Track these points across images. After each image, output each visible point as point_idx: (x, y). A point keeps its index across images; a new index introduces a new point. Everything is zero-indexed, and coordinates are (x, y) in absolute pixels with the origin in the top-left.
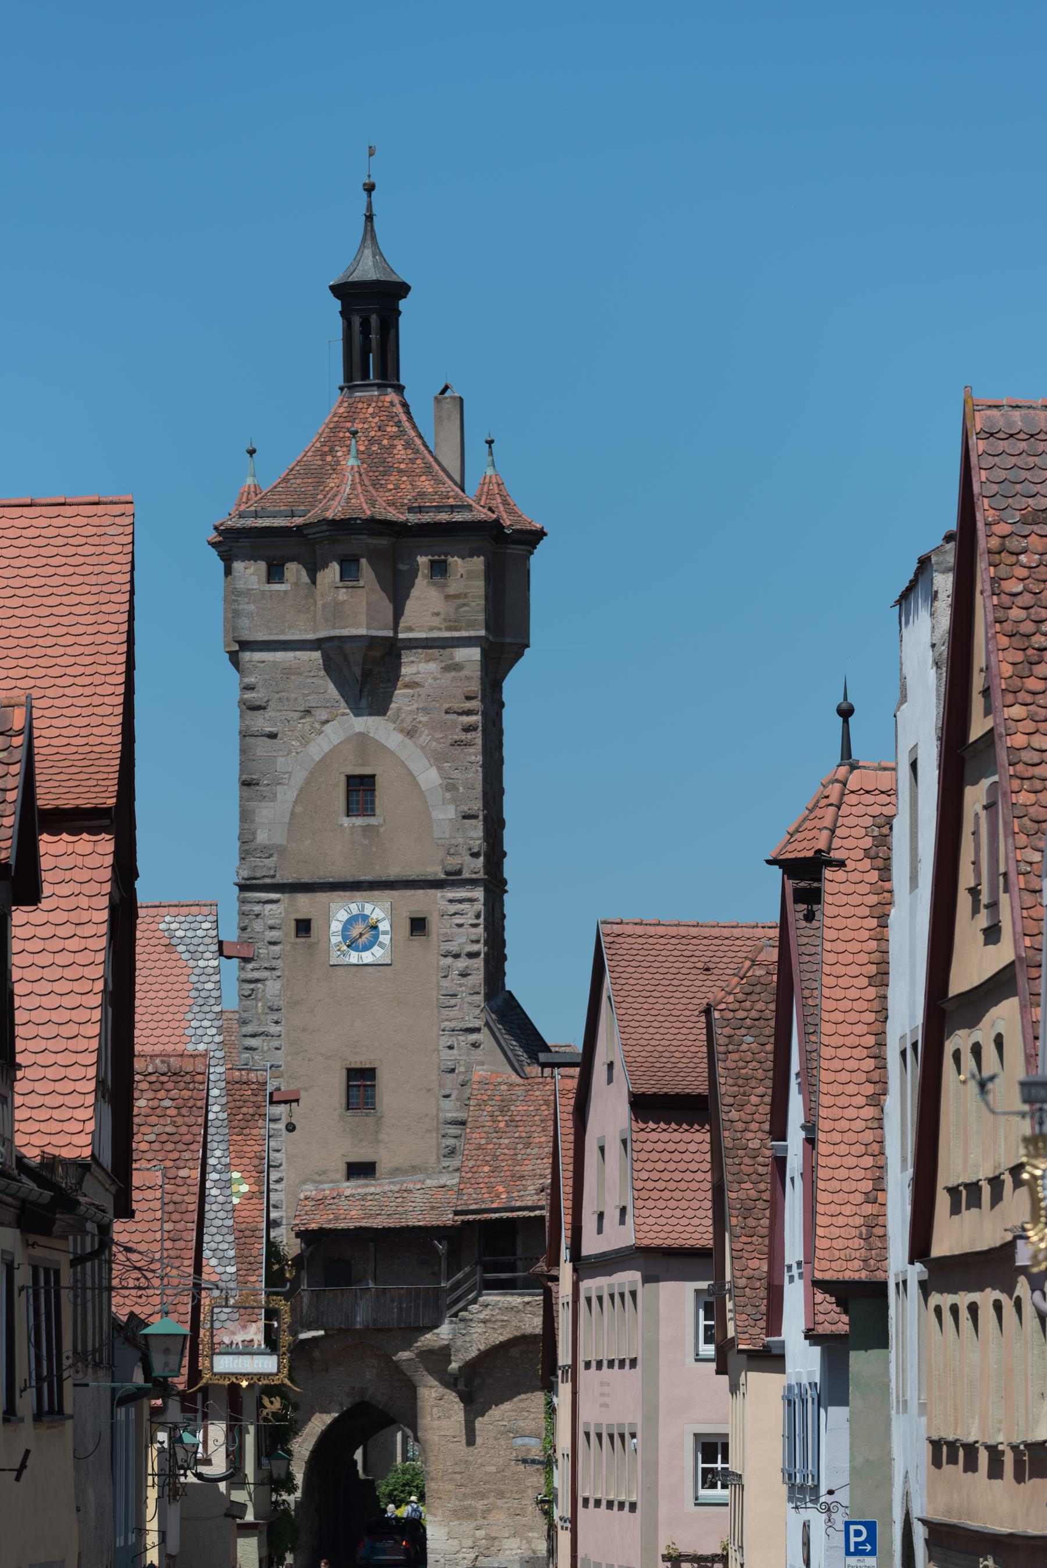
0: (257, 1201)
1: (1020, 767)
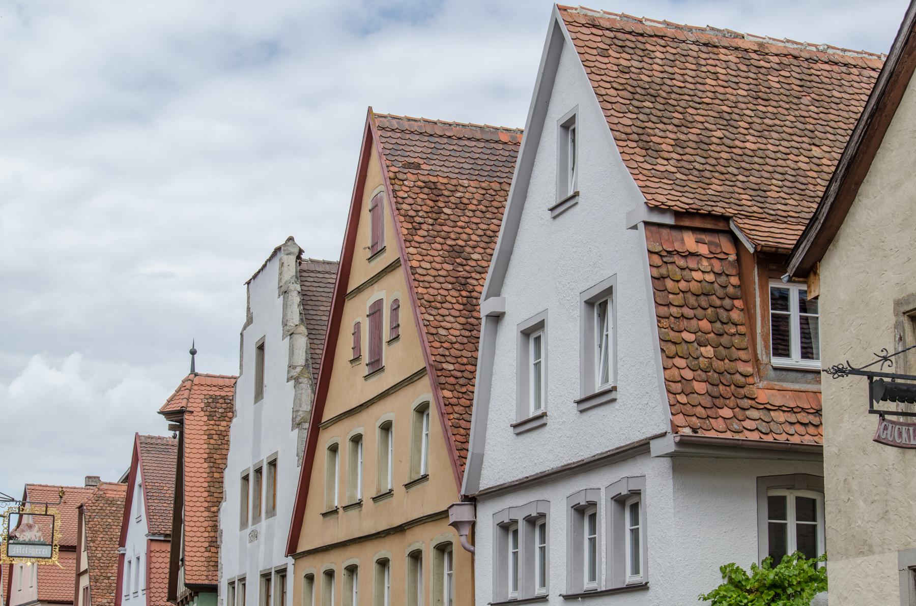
1: (417, 276)
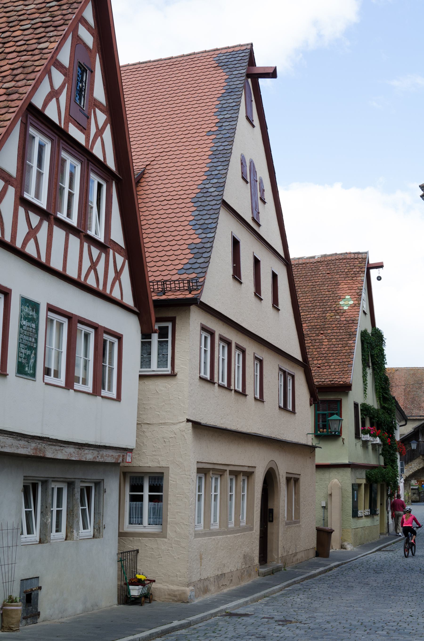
0: (357, 308)
